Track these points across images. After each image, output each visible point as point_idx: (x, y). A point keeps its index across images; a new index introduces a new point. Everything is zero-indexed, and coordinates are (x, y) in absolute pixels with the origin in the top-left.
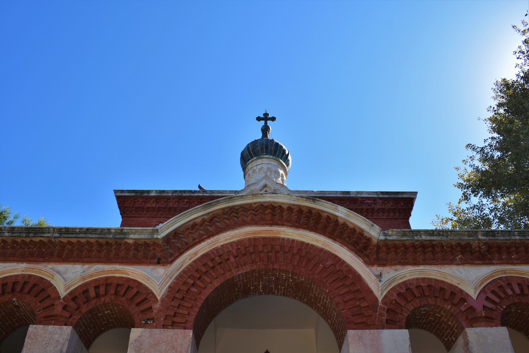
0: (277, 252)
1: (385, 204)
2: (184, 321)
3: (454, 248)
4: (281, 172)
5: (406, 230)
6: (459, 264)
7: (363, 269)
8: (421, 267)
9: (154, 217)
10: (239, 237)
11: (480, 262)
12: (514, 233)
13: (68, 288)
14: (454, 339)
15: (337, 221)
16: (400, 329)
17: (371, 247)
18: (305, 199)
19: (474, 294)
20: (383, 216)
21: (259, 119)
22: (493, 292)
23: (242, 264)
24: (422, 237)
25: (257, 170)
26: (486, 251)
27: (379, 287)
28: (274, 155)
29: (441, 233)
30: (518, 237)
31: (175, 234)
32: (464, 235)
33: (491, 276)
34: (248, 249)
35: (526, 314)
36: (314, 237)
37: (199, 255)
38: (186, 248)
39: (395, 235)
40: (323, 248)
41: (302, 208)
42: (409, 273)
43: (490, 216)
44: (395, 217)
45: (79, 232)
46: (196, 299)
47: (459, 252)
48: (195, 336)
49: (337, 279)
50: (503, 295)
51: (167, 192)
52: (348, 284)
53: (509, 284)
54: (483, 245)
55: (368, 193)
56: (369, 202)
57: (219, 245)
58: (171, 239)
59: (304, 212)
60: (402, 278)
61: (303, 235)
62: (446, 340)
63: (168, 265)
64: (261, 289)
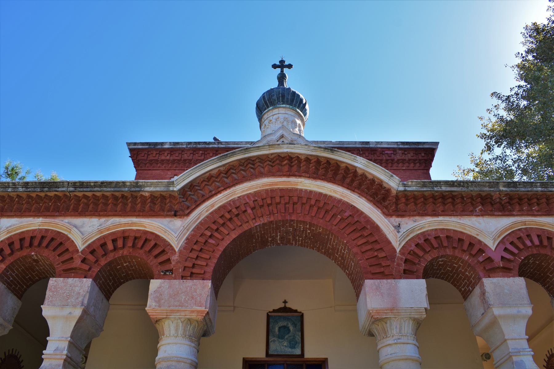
0: (294, 204)
1: (405, 154)
2: (203, 272)
3: (475, 199)
4: (298, 122)
5: (425, 181)
6: (479, 216)
7: (382, 220)
8: (441, 218)
9: (168, 170)
10: (256, 189)
11: (500, 213)
12: (537, 184)
13: (86, 242)
14: (471, 289)
15: (355, 172)
16: (417, 279)
17: (390, 198)
18: (323, 150)
19: (492, 245)
20: (403, 167)
21: (275, 66)
22: (512, 243)
23: (260, 216)
24: (442, 188)
25: (274, 120)
26: (506, 203)
27: (397, 238)
28: (291, 104)
29: (462, 184)
30: (540, 189)
31: (191, 186)
32: (485, 186)
33: (510, 227)
34: (265, 201)
35: (544, 265)
36: (332, 188)
37: (216, 207)
38: (202, 200)
39: (415, 186)
40: (341, 199)
41: (320, 159)
42: (427, 224)
43: (513, 168)
44: (415, 168)
45: (94, 185)
46: (214, 251)
47: (479, 204)
48: (213, 287)
49: (355, 230)
50: (521, 247)
51: (182, 143)
52: (366, 235)
53: (528, 236)
54: (503, 197)
55: (388, 143)
56: (389, 152)
57: (236, 196)
58: (187, 191)
59: (322, 163)
60: (421, 229)
61: (320, 186)
62: (463, 289)
63: (185, 217)
64: (278, 240)
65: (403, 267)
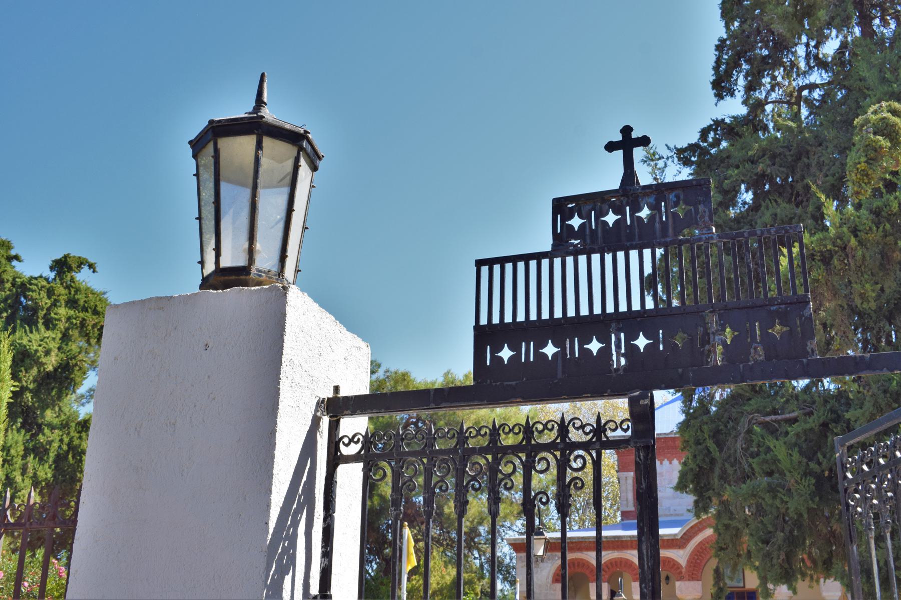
37: (698, 543)
57: (706, 536)
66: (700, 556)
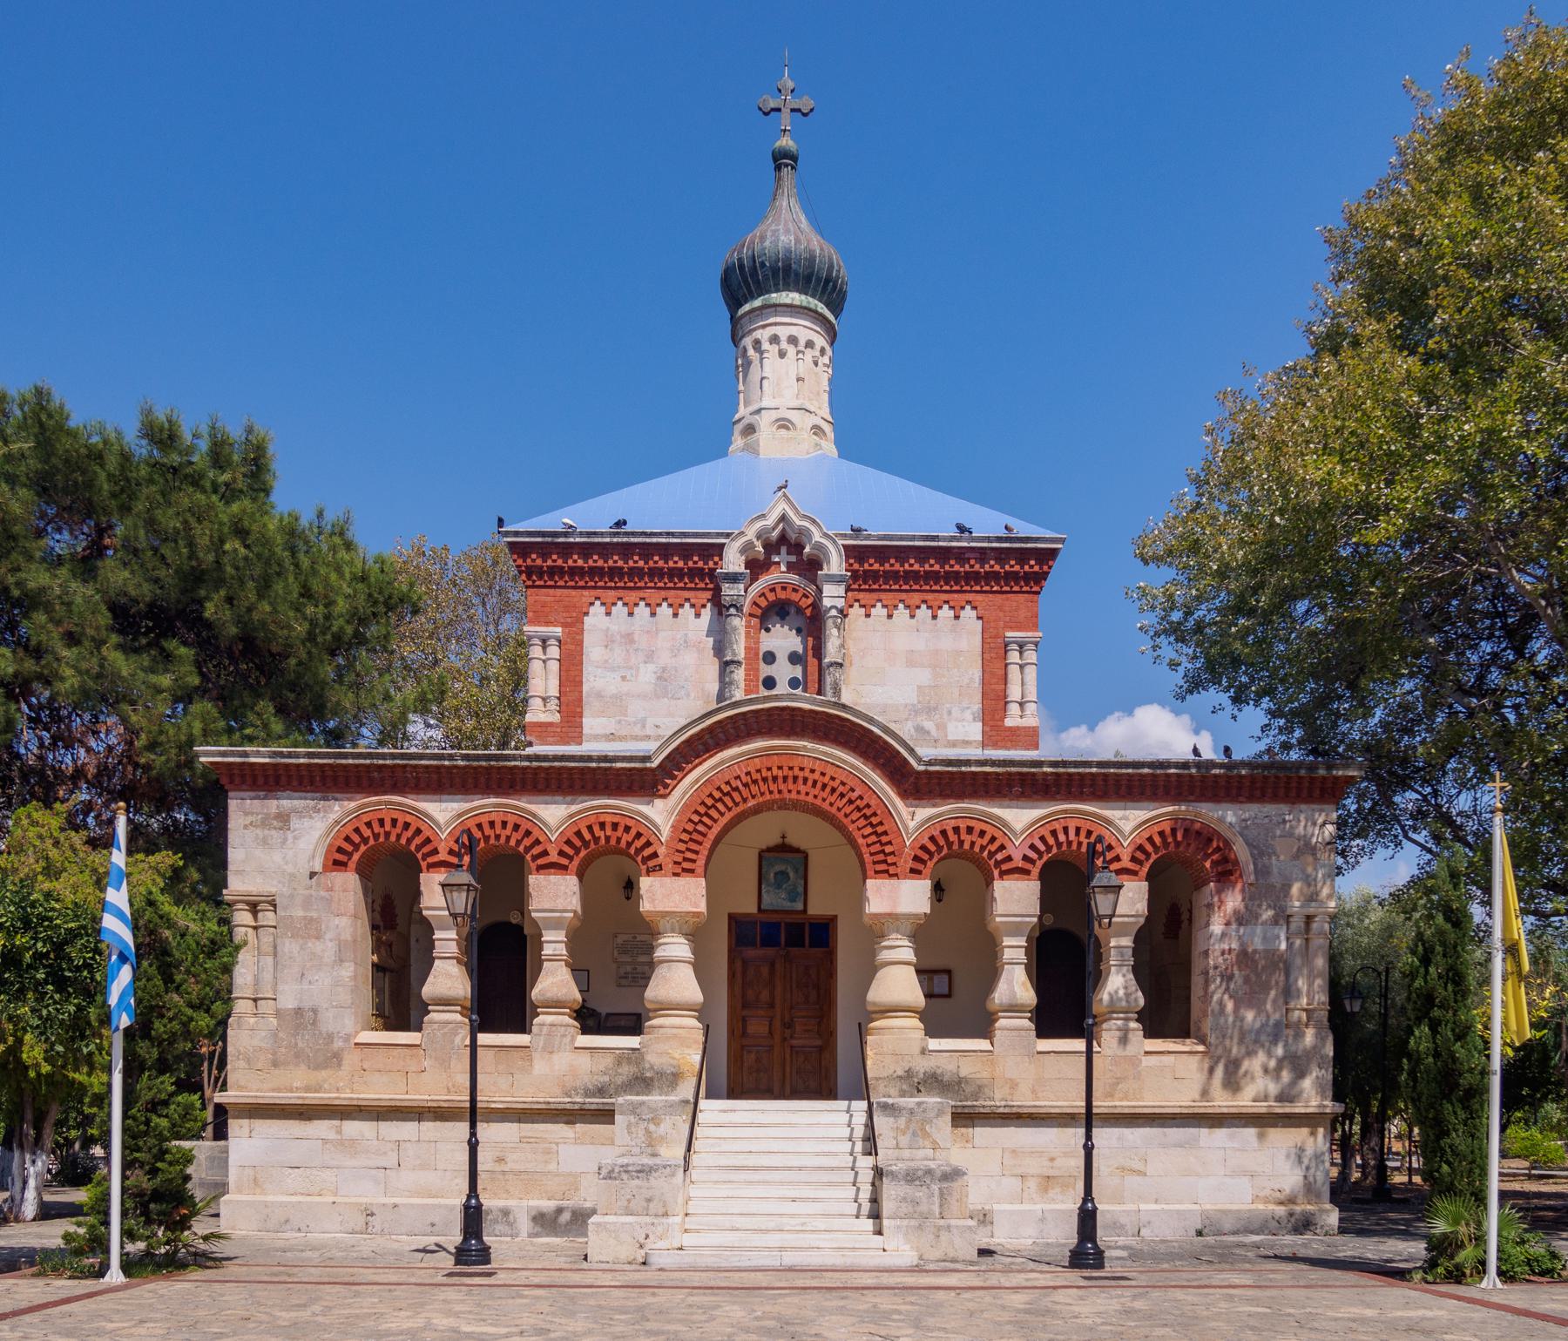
65: (910, 864)
66: (707, 814)
